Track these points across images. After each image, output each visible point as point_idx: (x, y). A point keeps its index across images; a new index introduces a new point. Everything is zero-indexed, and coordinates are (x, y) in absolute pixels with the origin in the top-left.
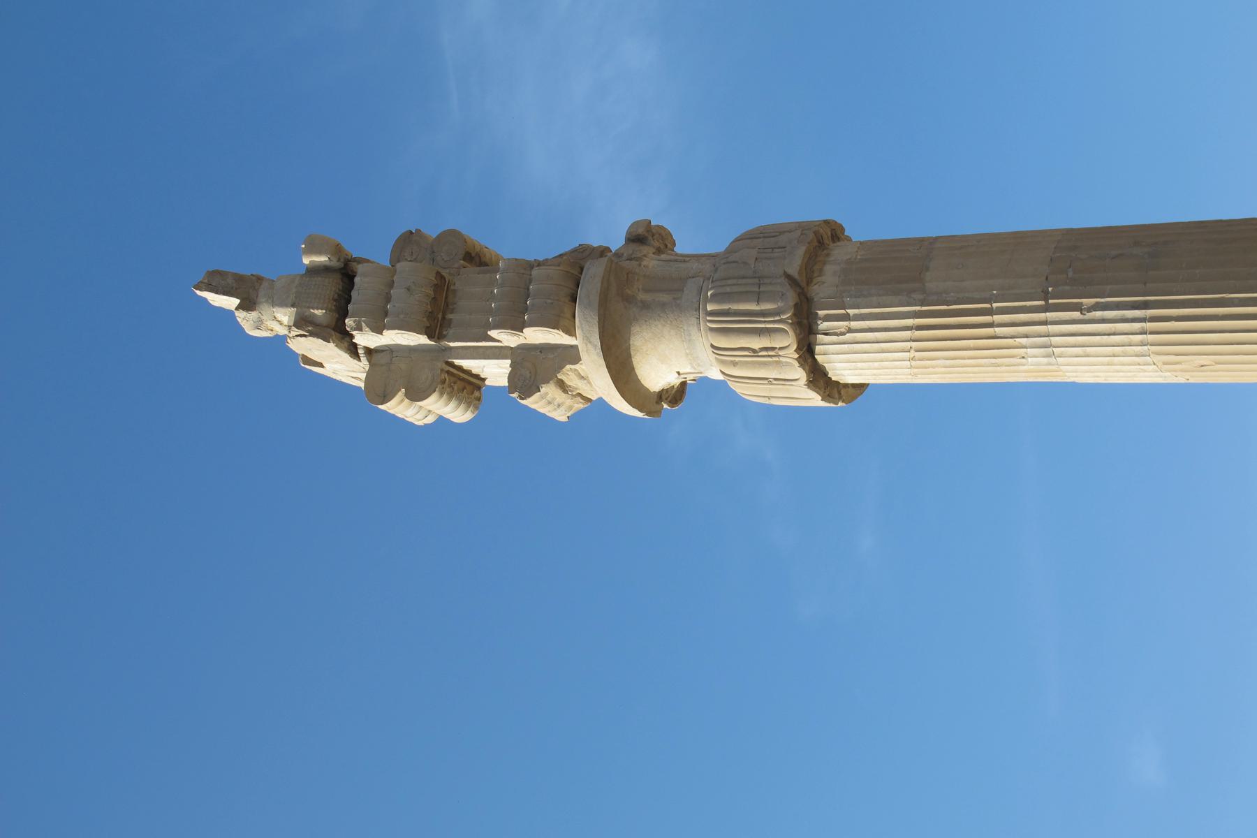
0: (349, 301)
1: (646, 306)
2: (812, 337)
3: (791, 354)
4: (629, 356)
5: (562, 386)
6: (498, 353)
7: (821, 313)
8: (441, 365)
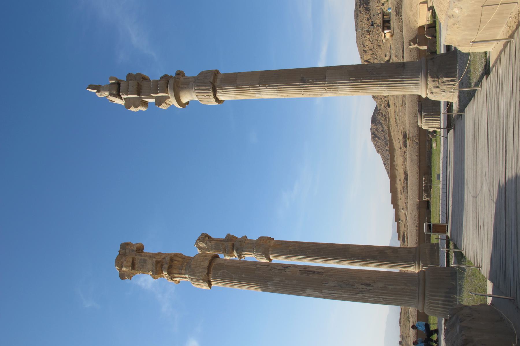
0: (120, 89)
1: (182, 88)
2: (216, 93)
3: (212, 96)
4: (180, 97)
5: (166, 103)
6: (152, 98)
7: (217, 88)
8: (140, 100)
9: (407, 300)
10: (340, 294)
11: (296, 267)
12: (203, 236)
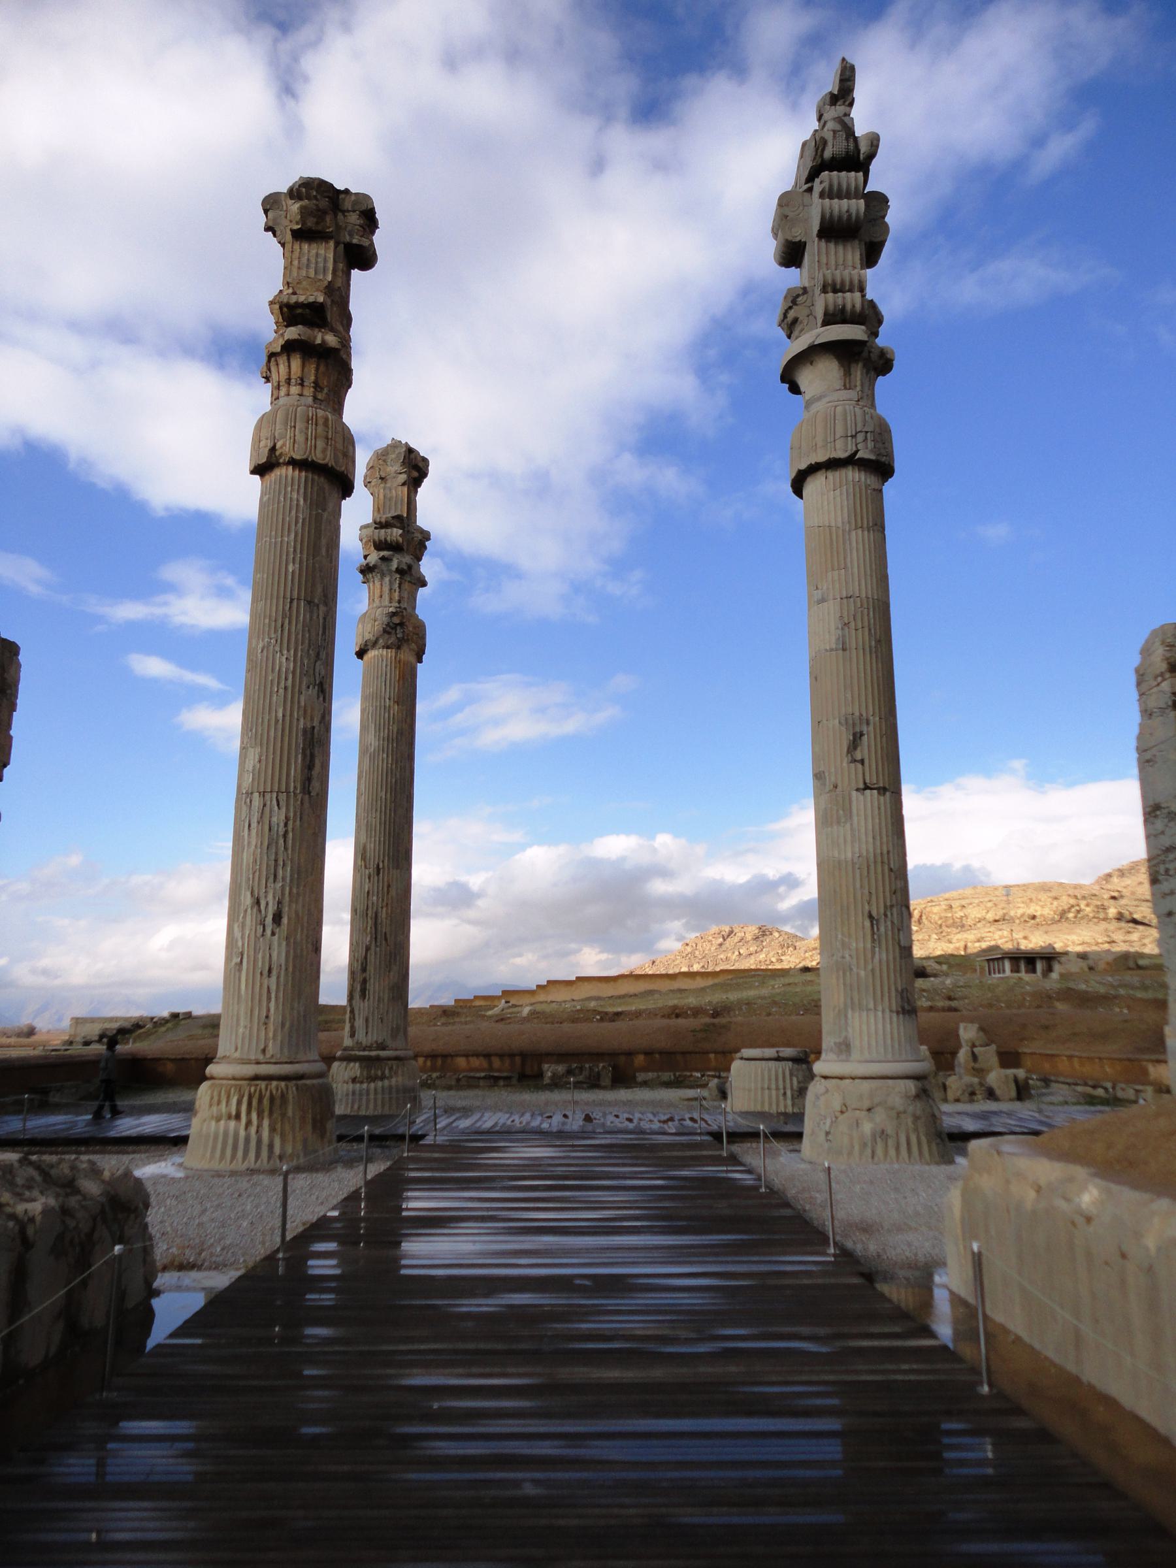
9: (237, 1031)
10: (249, 843)
11: (323, 717)
12: (421, 464)
